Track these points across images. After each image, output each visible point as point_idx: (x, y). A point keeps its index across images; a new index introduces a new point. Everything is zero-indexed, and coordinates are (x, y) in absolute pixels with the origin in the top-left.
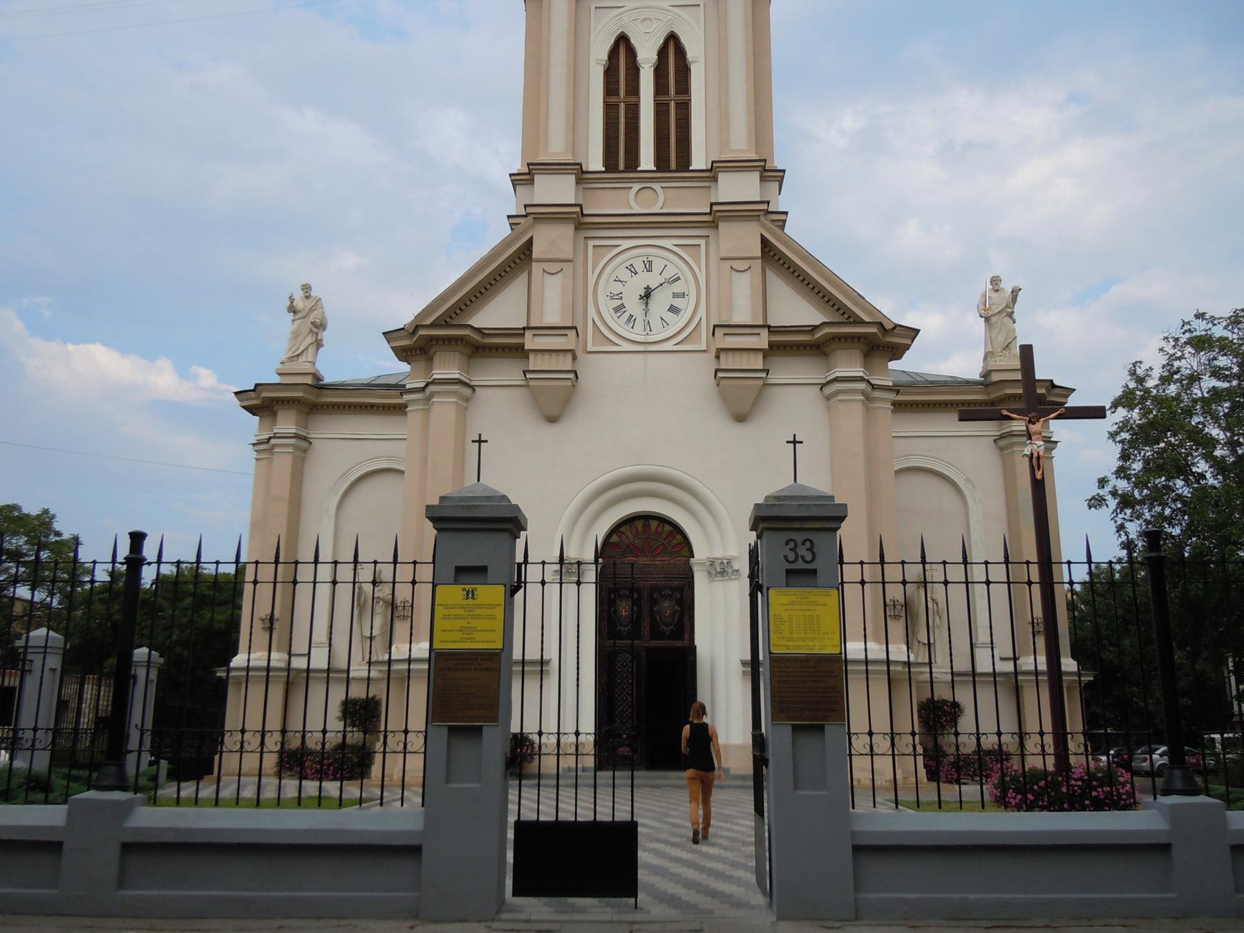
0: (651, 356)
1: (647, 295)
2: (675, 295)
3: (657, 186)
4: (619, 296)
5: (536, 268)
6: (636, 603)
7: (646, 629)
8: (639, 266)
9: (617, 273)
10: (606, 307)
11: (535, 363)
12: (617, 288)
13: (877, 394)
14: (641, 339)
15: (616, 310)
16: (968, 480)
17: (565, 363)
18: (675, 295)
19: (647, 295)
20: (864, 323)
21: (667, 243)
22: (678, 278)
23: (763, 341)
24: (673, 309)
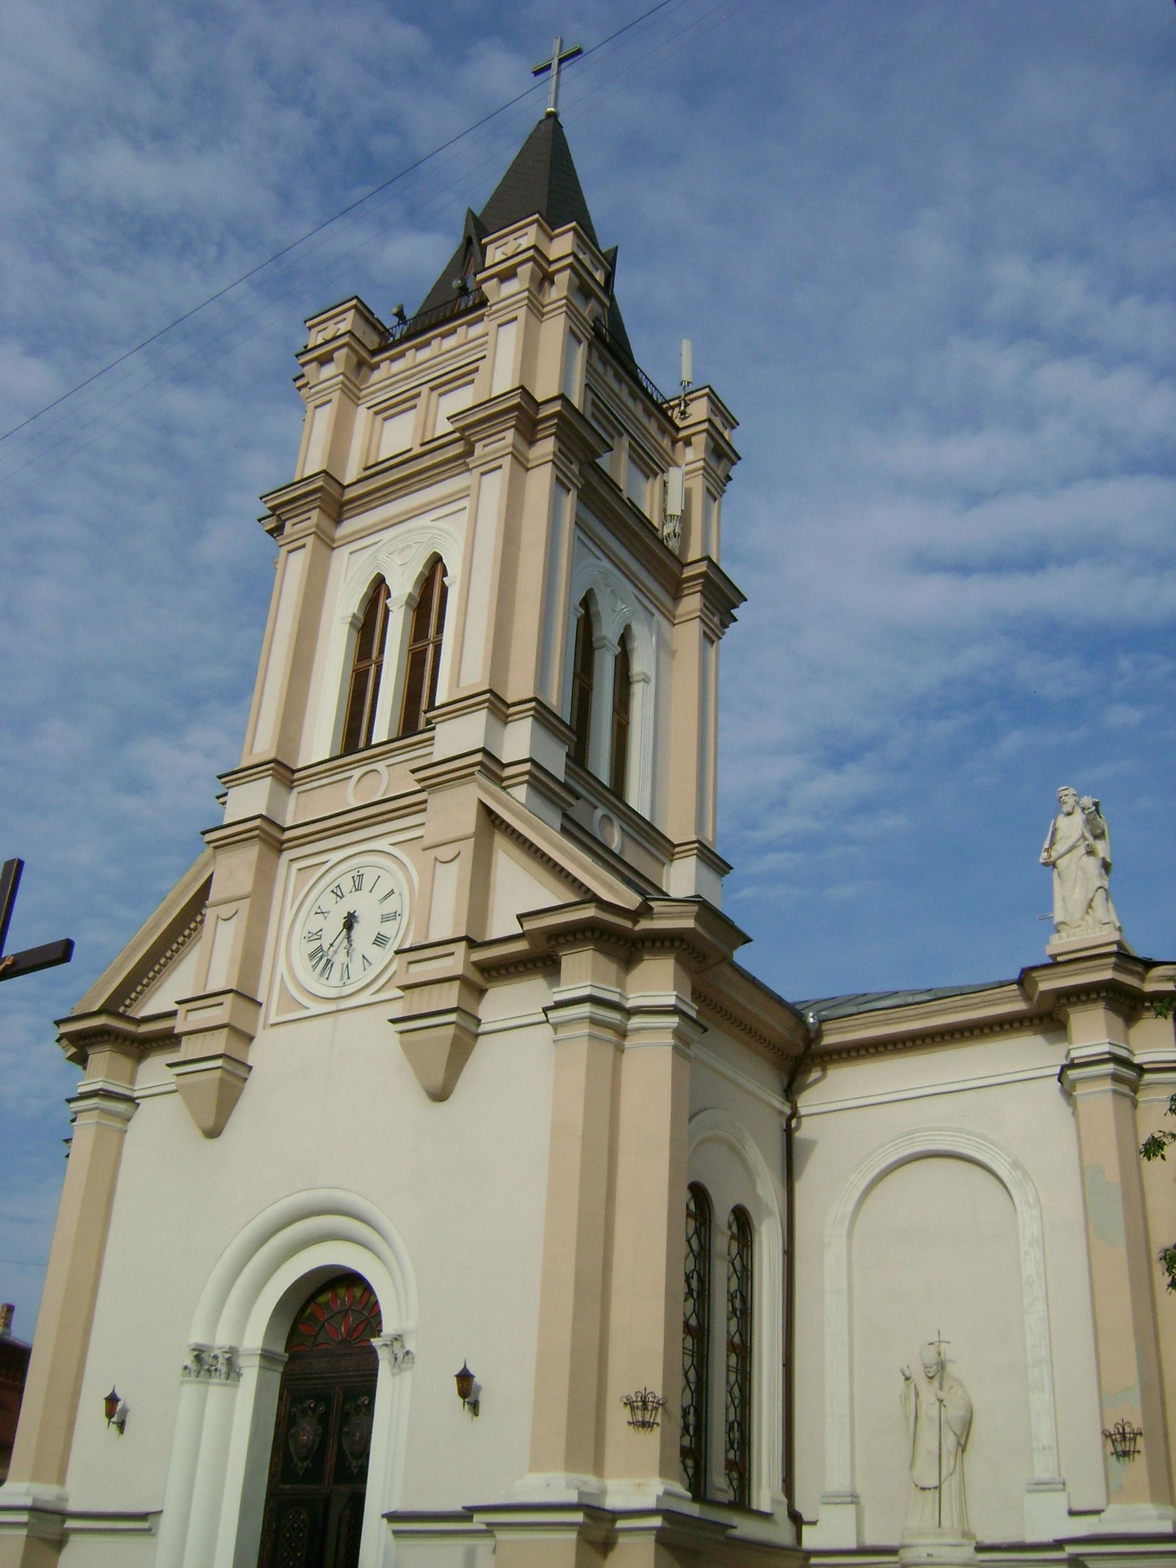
0: (343, 1017)
1: (350, 922)
2: (385, 918)
3: (380, 766)
4: (318, 935)
5: (210, 913)
6: (324, 1419)
7: (330, 1463)
8: (347, 884)
9: (321, 902)
10: (300, 950)
11: (189, 1049)
12: (316, 923)
13: (636, 1022)
14: (333, 993)
15: (312, 956)
16: (1016, 1165)
17: (218, 1043)
18: (385, 918)
19: (350, 922)
20: (595, 899)
21: (382, 844)
22: (392, 892)
23: (456, 962)
24: (380, 940)
